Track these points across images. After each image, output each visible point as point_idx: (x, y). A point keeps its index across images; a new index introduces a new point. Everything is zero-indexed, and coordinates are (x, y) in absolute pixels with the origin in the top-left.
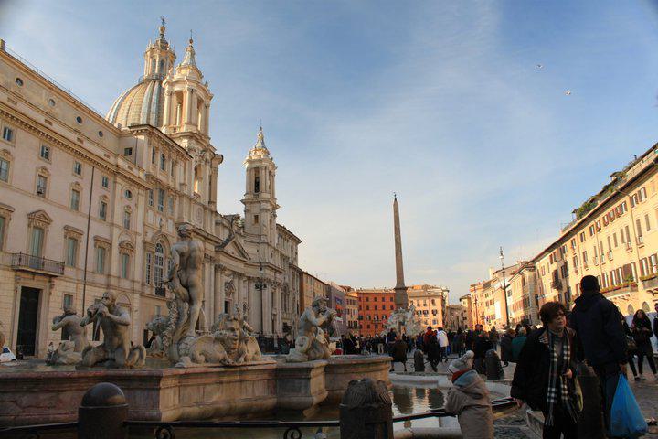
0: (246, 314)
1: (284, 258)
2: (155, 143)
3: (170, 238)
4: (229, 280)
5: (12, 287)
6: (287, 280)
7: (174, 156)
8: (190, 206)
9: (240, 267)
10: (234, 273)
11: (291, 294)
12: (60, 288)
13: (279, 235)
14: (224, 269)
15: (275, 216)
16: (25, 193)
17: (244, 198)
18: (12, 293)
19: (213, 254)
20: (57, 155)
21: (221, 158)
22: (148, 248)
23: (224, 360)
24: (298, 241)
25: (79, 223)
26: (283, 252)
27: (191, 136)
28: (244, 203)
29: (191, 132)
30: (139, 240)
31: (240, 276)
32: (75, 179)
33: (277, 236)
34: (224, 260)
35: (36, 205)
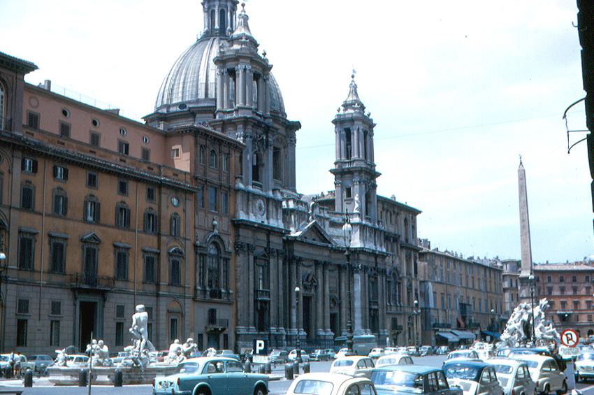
0: (336, 311)
1: (390, 238)
2: (202, 141)
3: (225, 238)
4: (310, 271)
5: (72, 303)
6: (397, 261)
7: (225, 149)
8: (248, 200)
9: (323, 256)
10: (317, 263)
11: (405, 282)
12: (113, 301)
13: (383, 209)
14: (300, 259)
15: (375, 186)
16: (79, 221)
17: (333, 167)
18: (72, 308)
19: (281, 248)
20: (102, 180)
21: (297, 126)
22: (199, 251)
23: (133, 365)
24: (415, 212)
25: (123, 238)
26: (392, 229)
27: (246, 121)
28: (334, 174)
29: (245, 118)
30: (189, 244)
31: (325, 265)
32: (120, 198)
33: (380, 209)
34: (299, 251)
35: (89, 231)
